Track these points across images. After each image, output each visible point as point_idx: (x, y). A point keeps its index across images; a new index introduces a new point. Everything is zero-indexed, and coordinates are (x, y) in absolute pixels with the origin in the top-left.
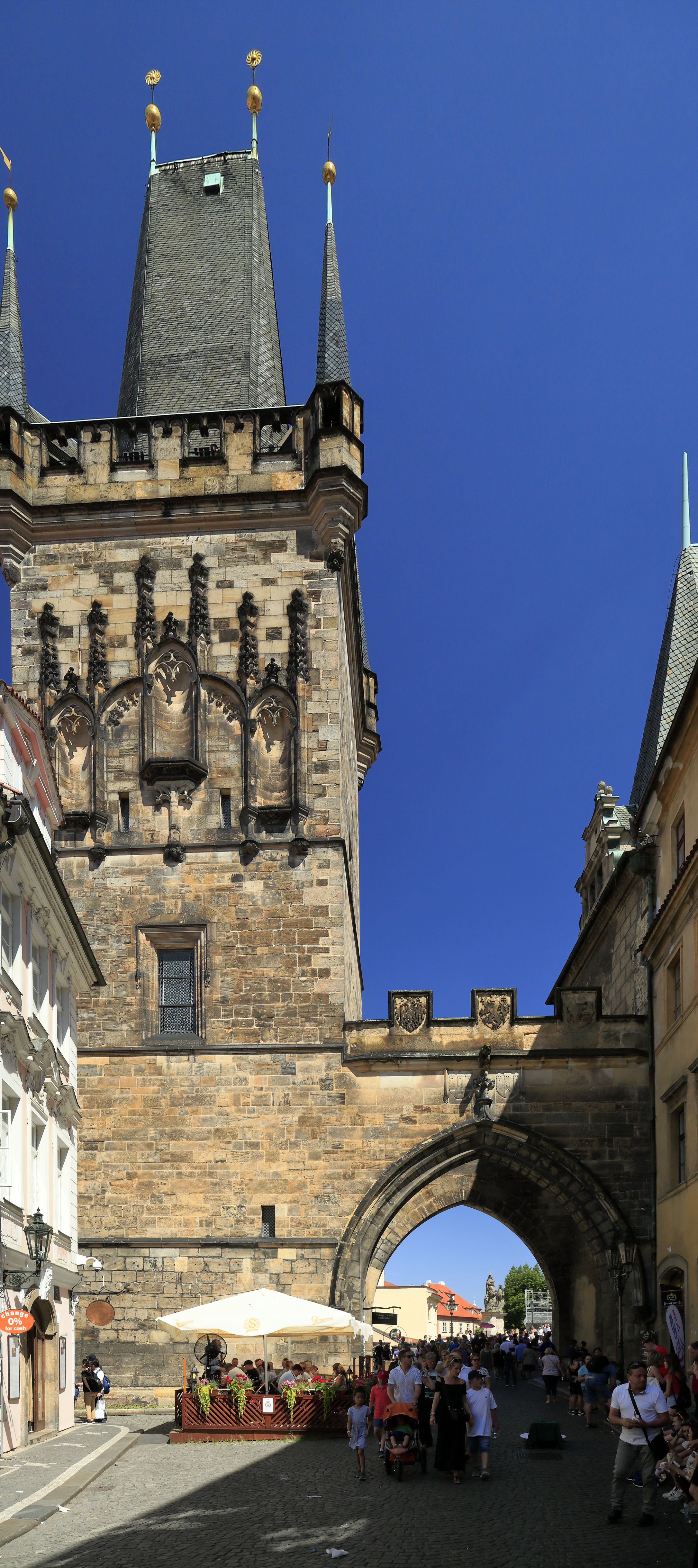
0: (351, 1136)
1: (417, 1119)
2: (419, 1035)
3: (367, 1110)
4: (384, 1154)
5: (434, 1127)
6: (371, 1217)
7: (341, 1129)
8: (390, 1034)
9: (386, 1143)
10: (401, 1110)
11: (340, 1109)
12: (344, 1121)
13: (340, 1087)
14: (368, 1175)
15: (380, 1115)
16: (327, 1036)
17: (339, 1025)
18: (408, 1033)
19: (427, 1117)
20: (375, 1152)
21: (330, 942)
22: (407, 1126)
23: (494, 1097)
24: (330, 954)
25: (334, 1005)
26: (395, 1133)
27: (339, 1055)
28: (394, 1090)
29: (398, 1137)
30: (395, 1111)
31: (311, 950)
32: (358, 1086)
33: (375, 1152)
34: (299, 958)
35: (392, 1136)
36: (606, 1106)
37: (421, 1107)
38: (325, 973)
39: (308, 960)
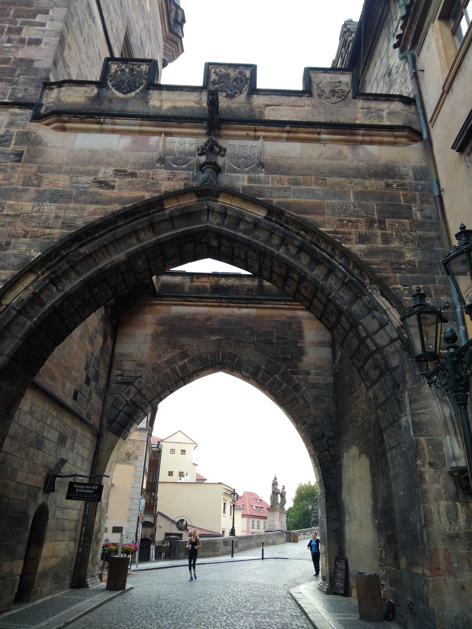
0: (18, 198)
1: (116, 185)
2: (134, 98)
3: (50, 171)
4: (60, 221)
5: (138, 194)
6: (19, 303)
7: (7, 189)
8: (98, 95)
9: (68, 209)
10: (97, 172)
11: (13, 168)
12: (14, 181)
13: (20, 144)
14: (30, 247)
15: (67, 177)
16: (20, 95)
17: (38, 87)
18: (121, 95)
19: (131, 183)
20: (48, 219)
21: (49, 18)
22: (101, 191)
23: (224, 165)
24: (47, 27)
25: (38, 69)
26: (83, 198)
27: (29, 112)
28: (91, 151)
29: (85, 202)
30: (88, 173)
31: (23, 23)
32: (46, 145)
33: (48, 219)
34: (9, 28)
35: (77, 201)
36: (376, 185)
37: (125, 171)
38: (37, 42)
39: (19, 31)
